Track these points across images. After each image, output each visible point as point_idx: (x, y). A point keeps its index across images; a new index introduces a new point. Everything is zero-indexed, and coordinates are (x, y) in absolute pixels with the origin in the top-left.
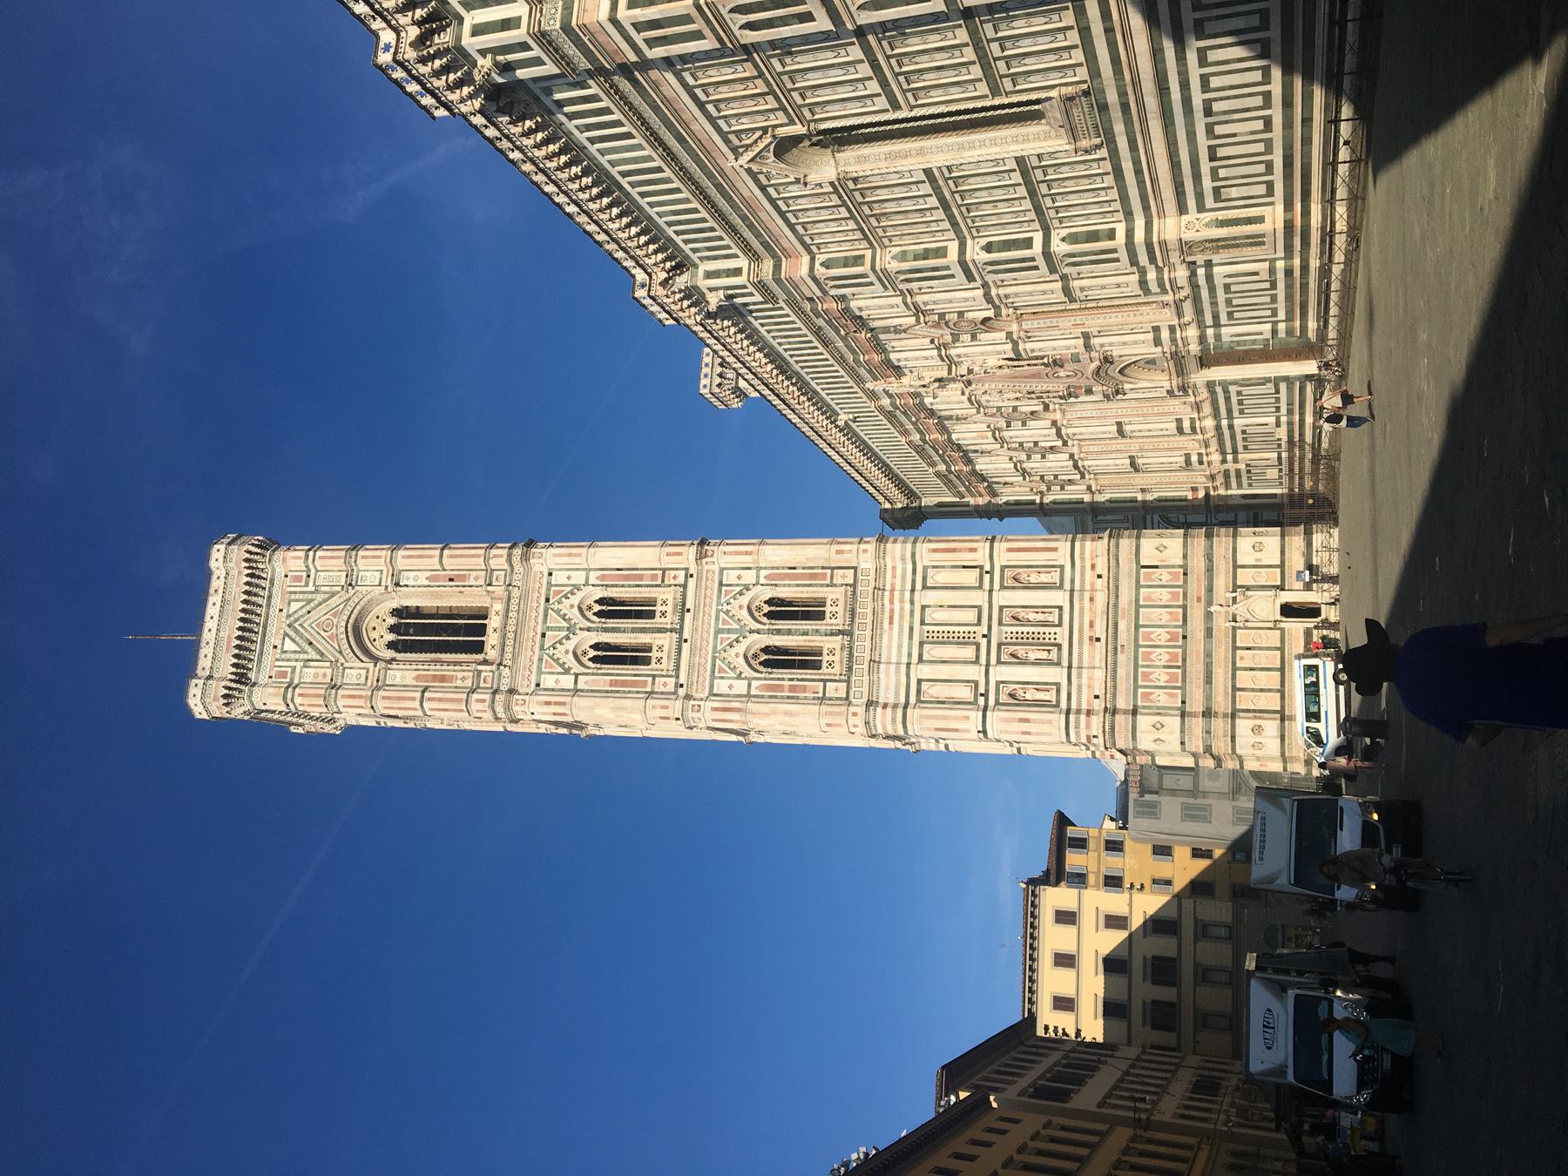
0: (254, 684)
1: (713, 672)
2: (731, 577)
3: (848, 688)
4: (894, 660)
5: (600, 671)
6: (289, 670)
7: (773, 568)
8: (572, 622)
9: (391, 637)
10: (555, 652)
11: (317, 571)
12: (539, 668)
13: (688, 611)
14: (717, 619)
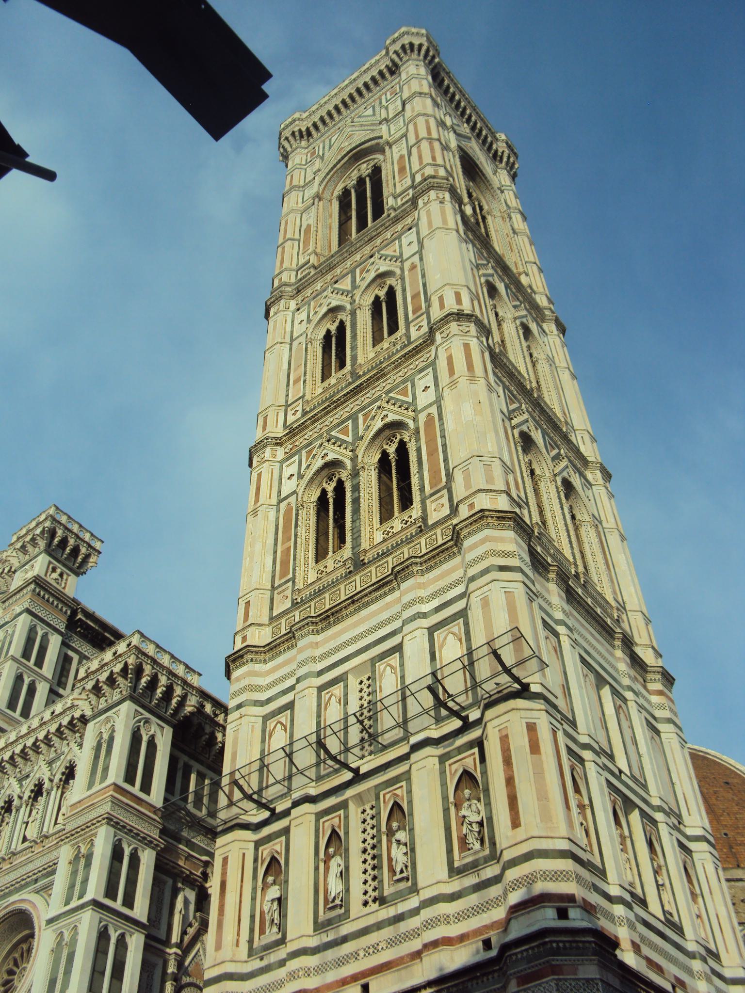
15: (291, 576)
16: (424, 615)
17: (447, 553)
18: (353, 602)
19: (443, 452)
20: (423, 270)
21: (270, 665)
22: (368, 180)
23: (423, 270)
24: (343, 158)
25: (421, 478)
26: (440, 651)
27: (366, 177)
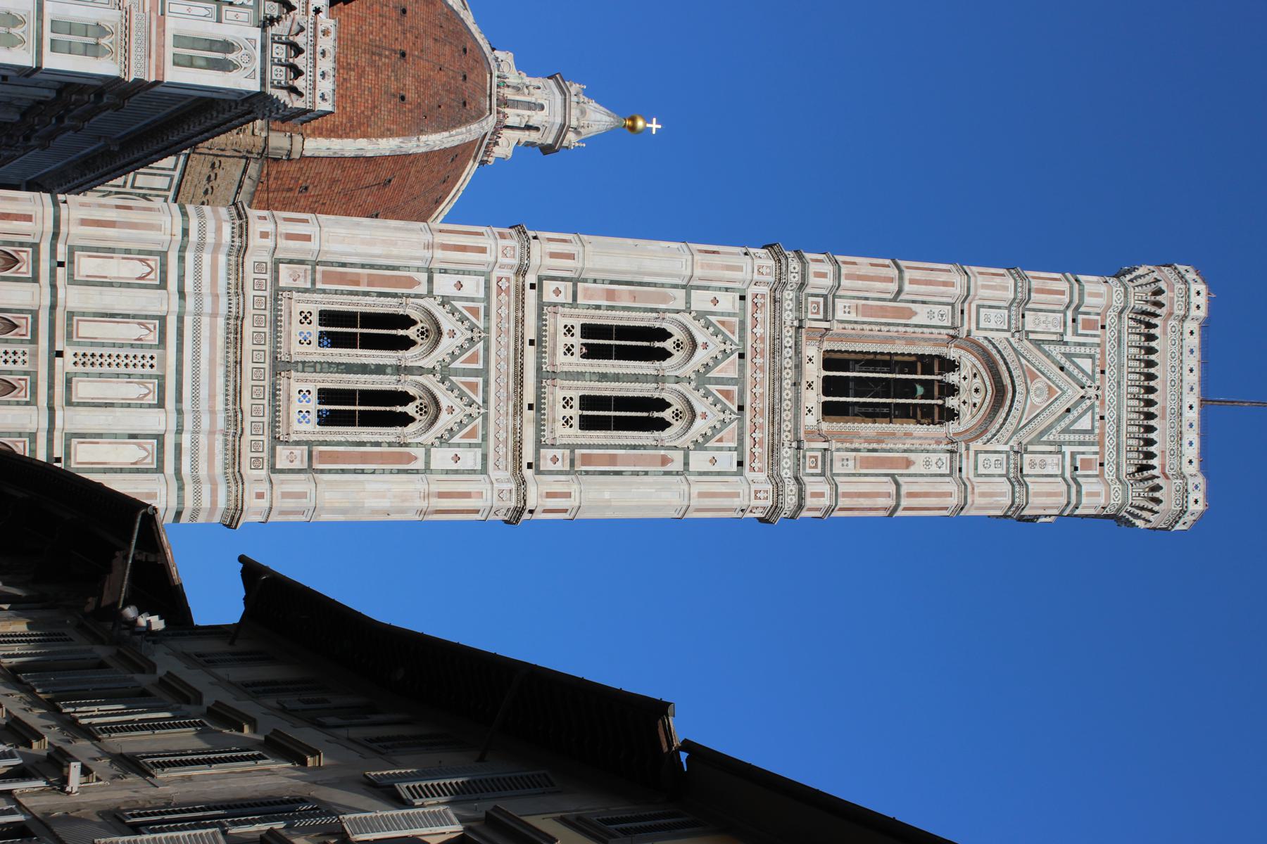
0: (1121, 312)
1: (487, 315)
2: (471, 459)
3: (276, 279)
4: (205, 320)
5: (655, 315)
6: (1080, 331)
7: (406, 472)
8: (702, 391)
9: (952, 378)
10: (722, 347)
11: (1063, 476)
12: (742, 324)
13: (530, 407)
14: (486, 392)
15: (319, 286)
16: (179, 431)
17: (231, 462)
18: (236, 362)
19: (355, 469)
20: (646, 473)
21: (222, 259)
22: (940, 402)
23: (646, 473)
24: (1011, 377)
25: (339, 444)
26: (134, 443)
27: (945, 401)
